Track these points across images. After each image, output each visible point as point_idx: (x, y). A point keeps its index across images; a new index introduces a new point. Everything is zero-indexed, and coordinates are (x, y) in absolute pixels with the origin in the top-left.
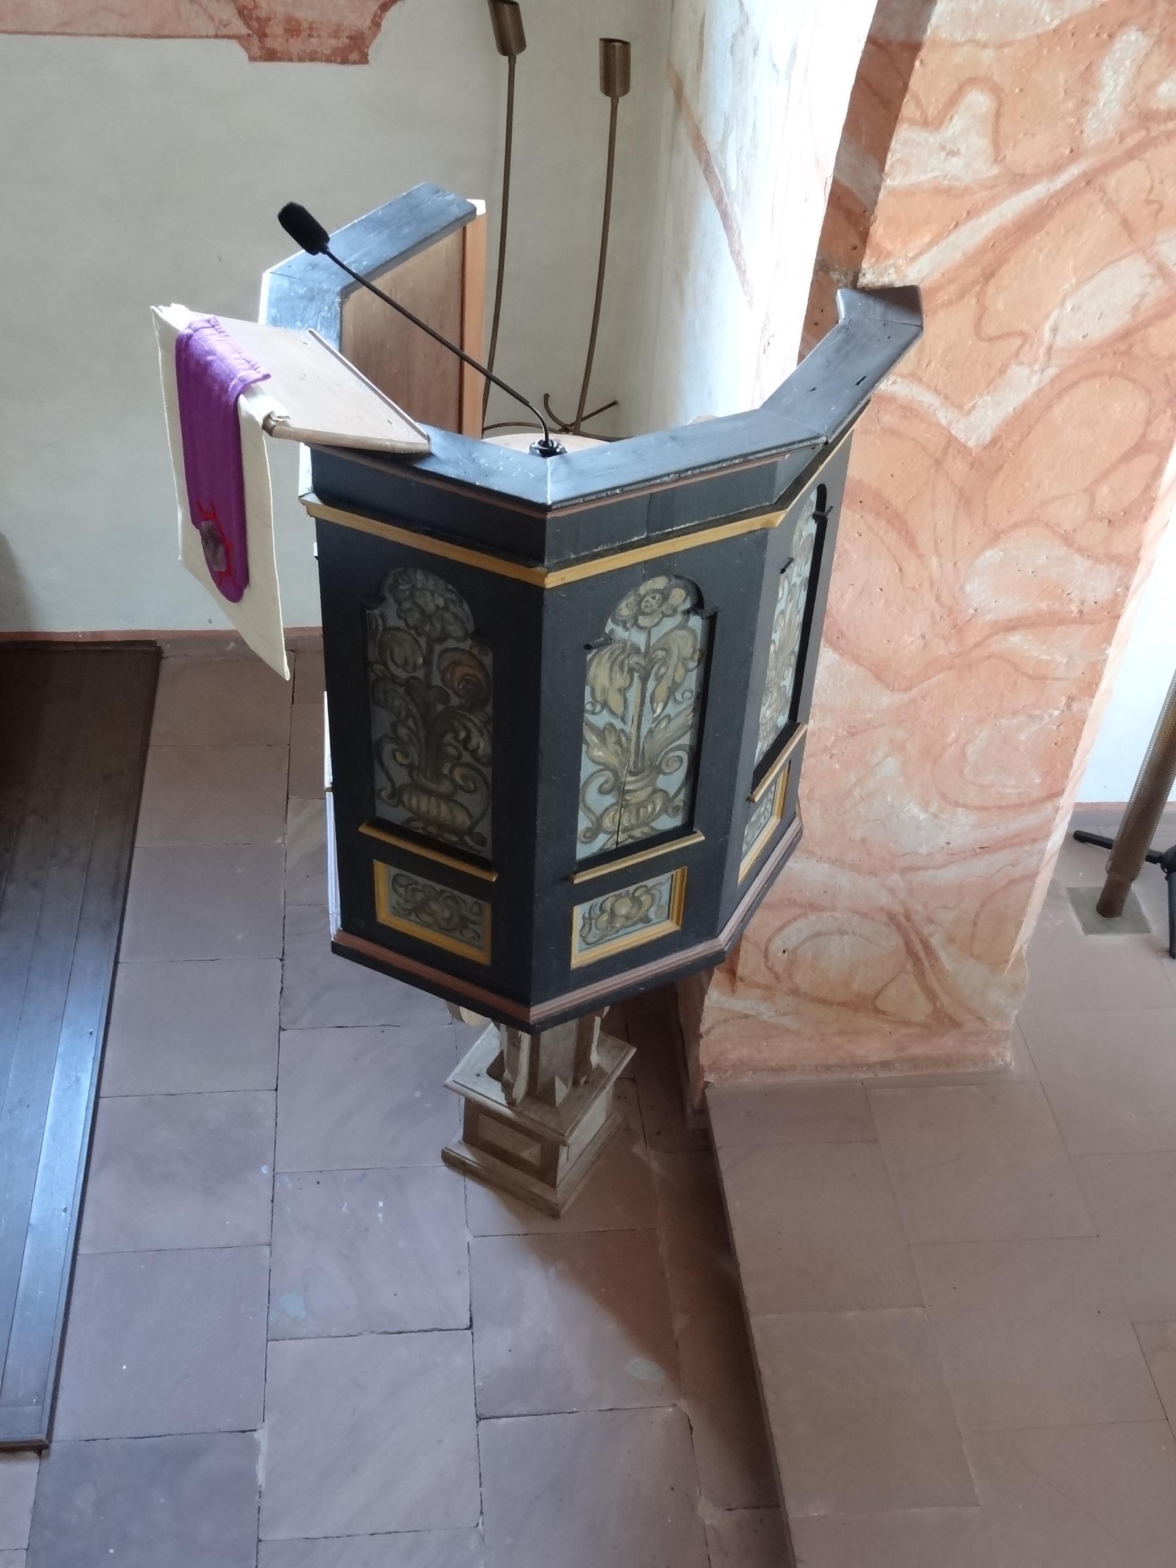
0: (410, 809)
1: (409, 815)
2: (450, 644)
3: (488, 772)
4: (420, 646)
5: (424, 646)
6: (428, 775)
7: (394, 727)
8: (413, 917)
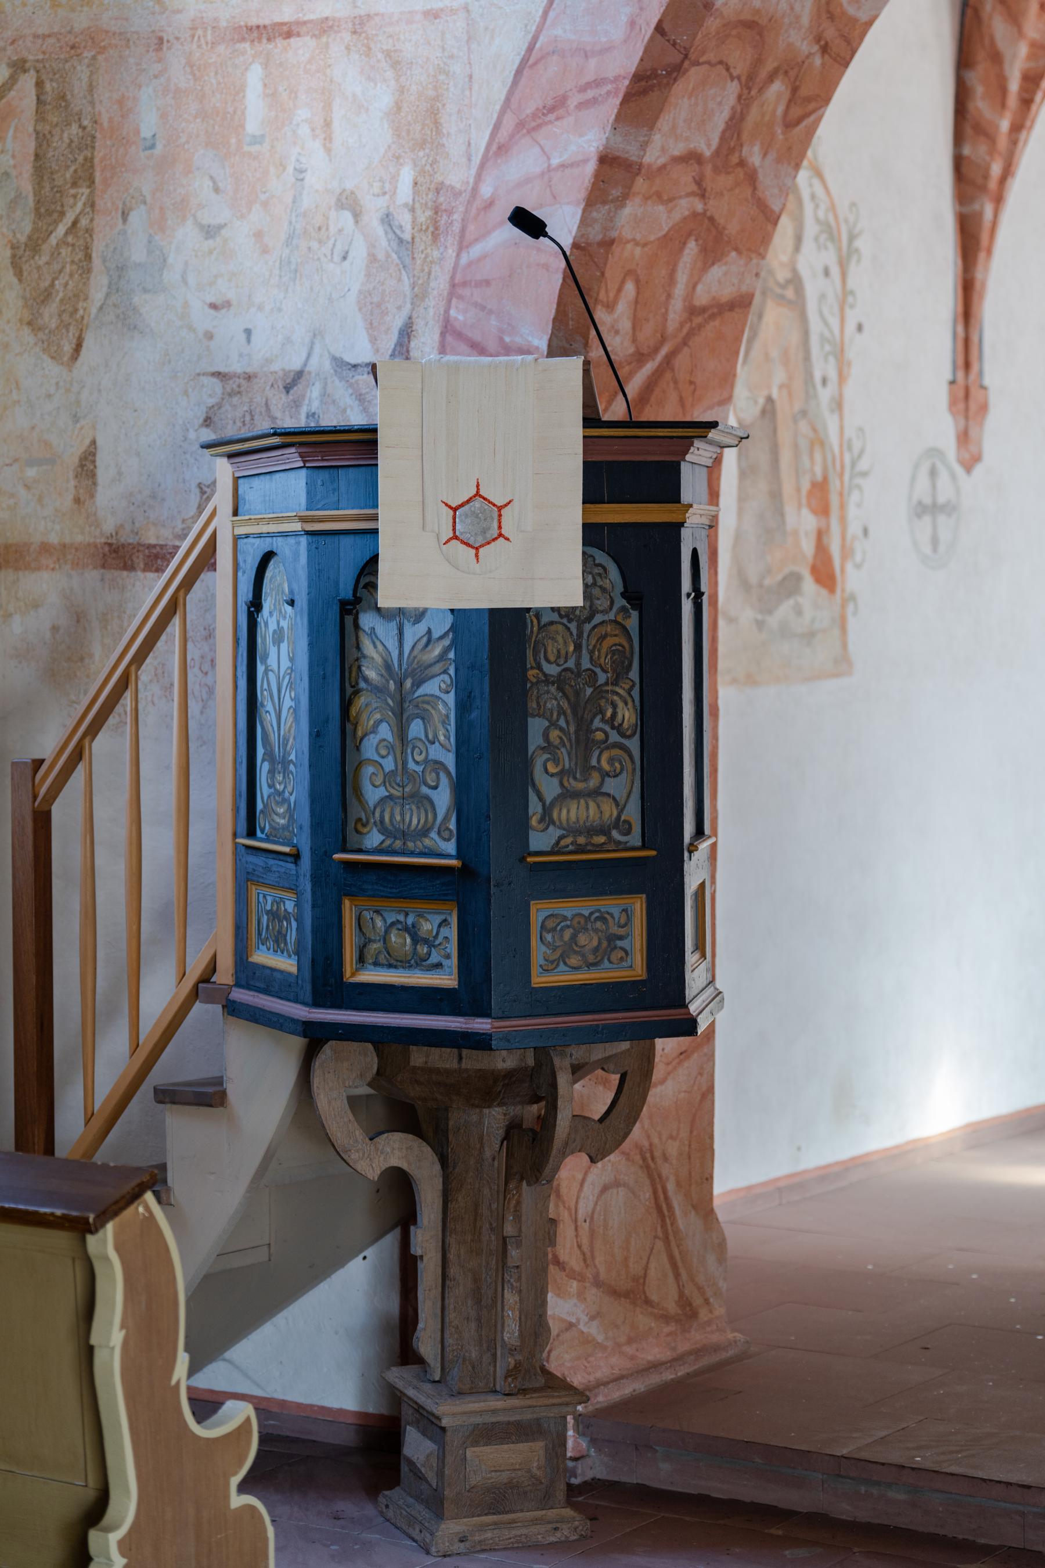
0: (561, 827)
1: (559, 832)
2: (598, 618)
3: (634, 745)
4: (571, 634)
5: (574, 632)
6: (578, 776)
7: (546, 735)
8: (562, 967)
